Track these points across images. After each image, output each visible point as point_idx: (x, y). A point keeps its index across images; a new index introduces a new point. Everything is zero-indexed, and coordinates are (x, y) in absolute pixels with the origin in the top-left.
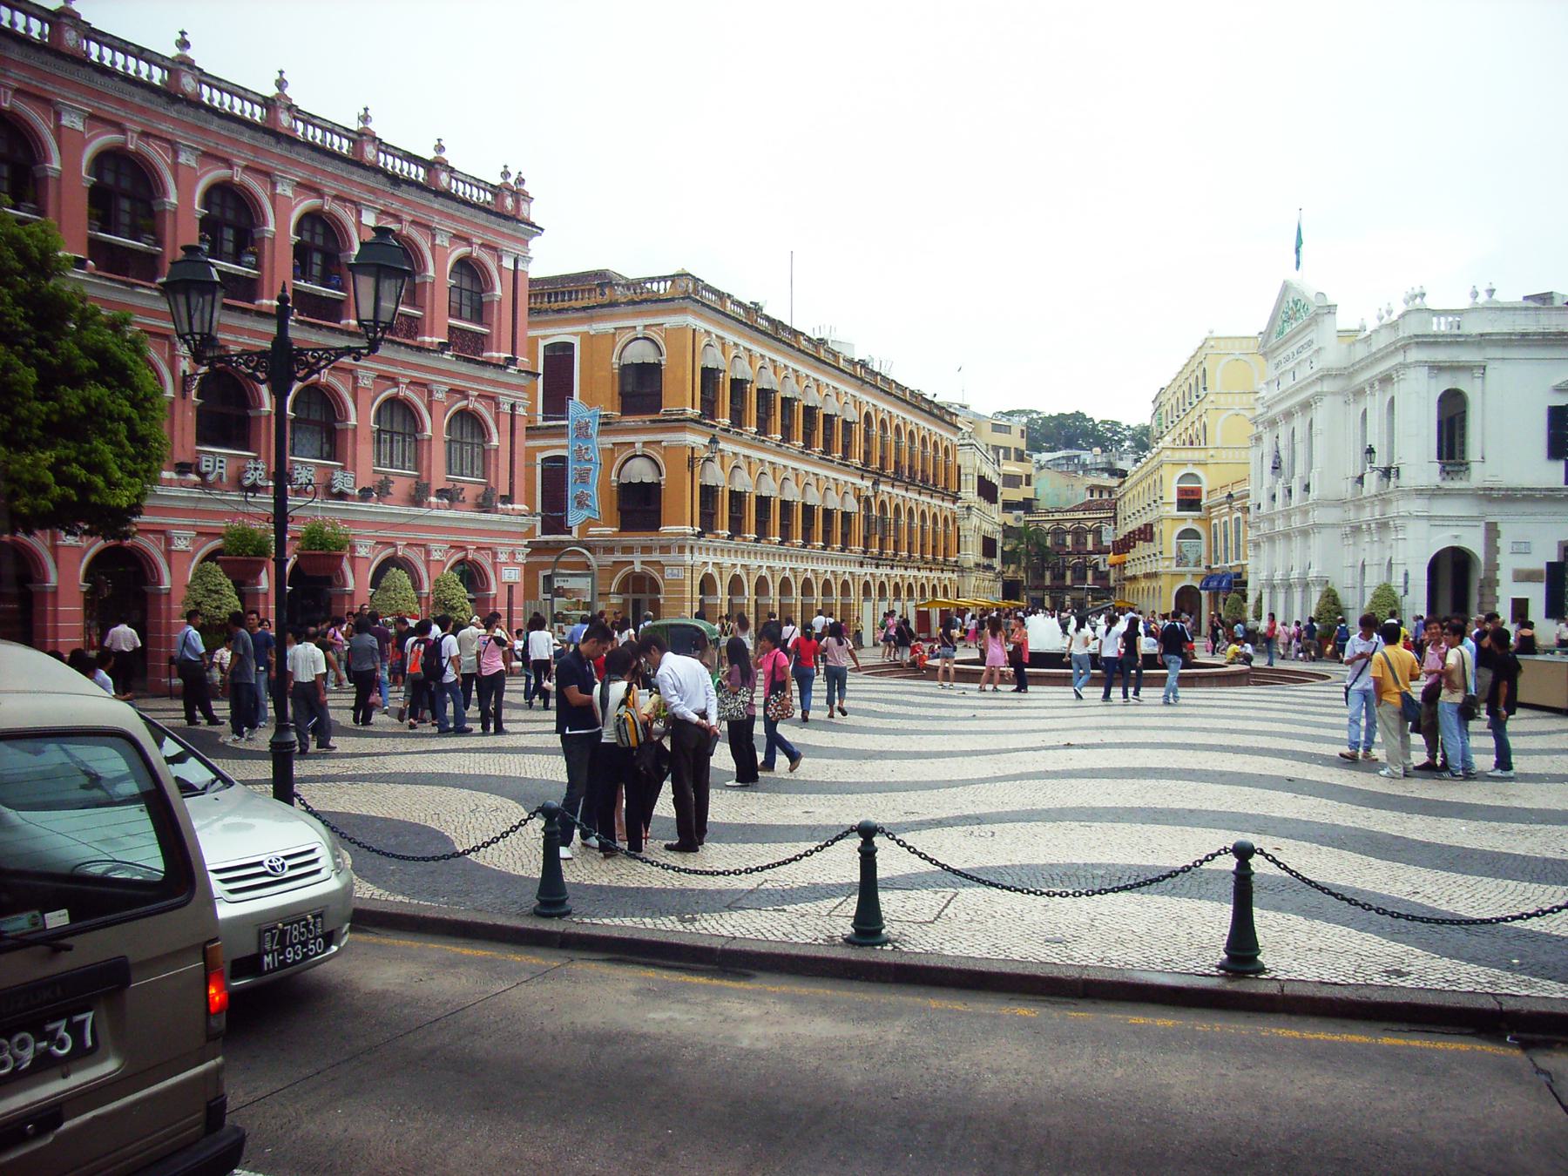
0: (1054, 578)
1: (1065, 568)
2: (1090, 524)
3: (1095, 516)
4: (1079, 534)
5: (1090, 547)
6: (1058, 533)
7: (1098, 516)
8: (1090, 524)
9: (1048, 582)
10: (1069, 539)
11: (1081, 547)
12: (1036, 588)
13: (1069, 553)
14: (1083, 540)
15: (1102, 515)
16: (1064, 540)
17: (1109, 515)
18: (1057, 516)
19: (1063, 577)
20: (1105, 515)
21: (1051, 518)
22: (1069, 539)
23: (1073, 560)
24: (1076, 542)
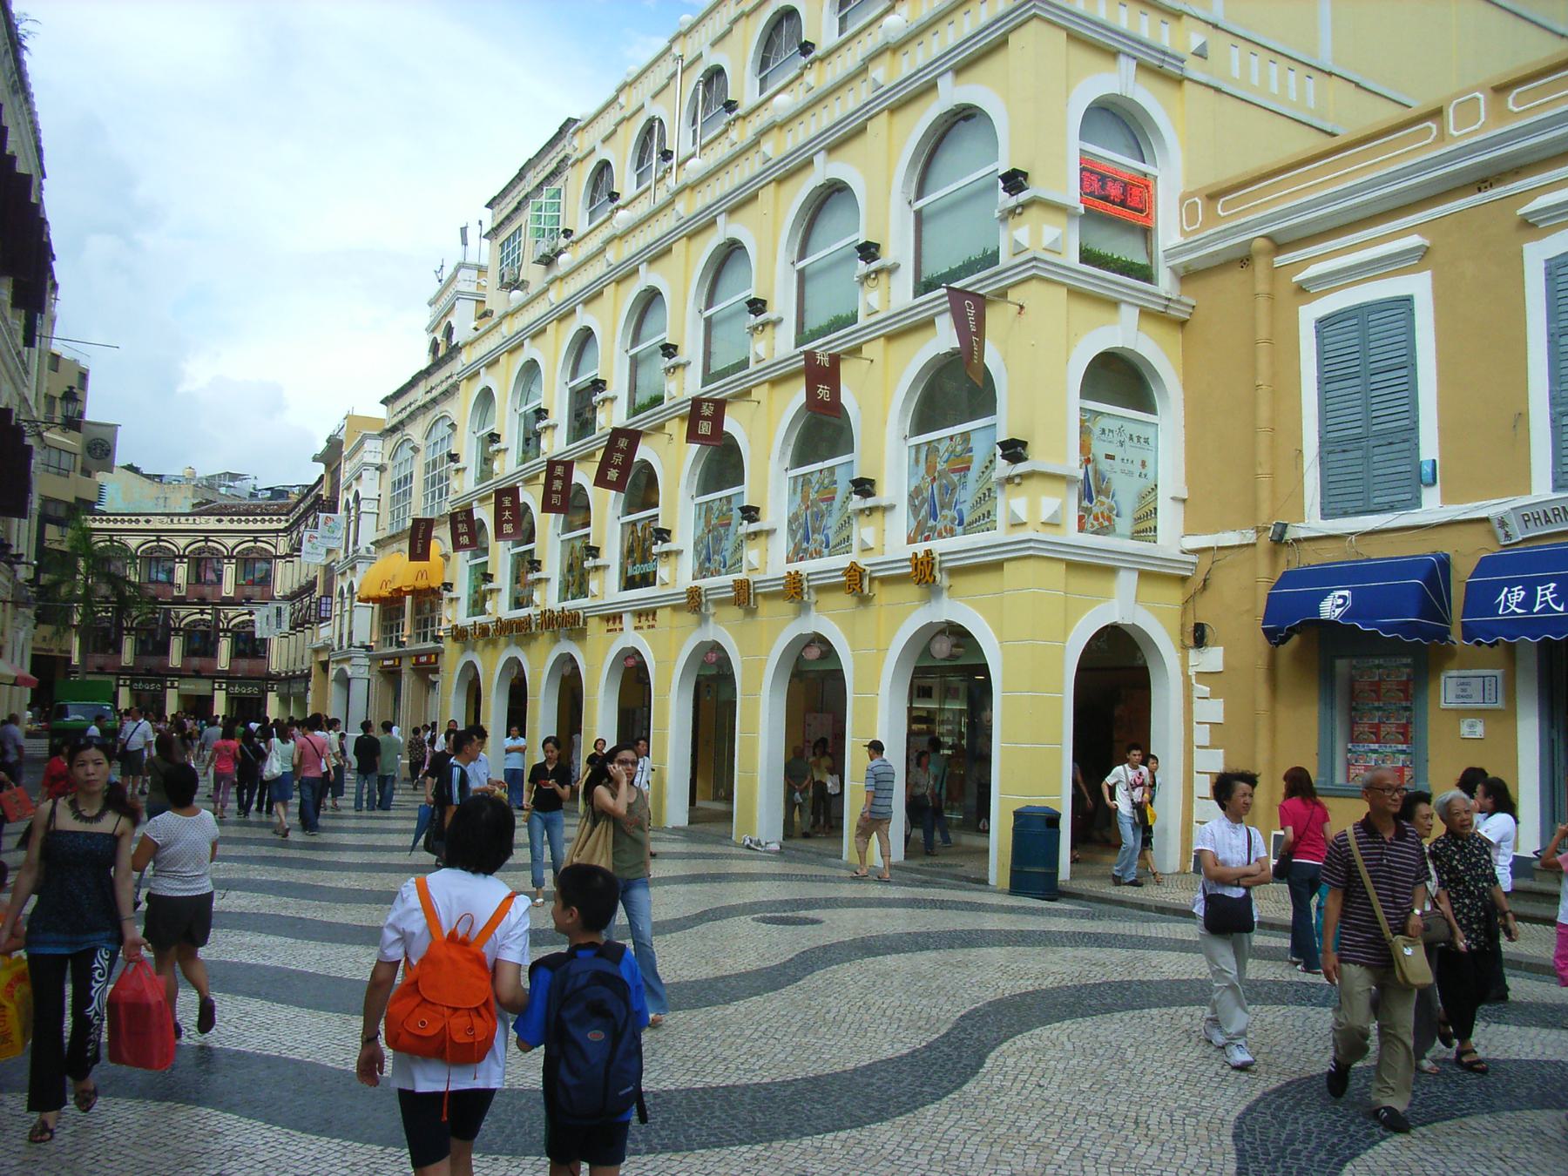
0: (141, 650)
1: (169, 631)
2: (230, 542)
3: (243, 526)
4: (203, 562)
5: (228, 589)
6: (159, 558)
7: (251, 526)
8: (230, 542)
9: (127, 657)
10: (181, 572)
11: (207, 590)
12: (198, 674)
13: (181, 601)
14: (211, 576)
15: (259, 526)
16: (171, 571)
17: (275, 526)
18: (156, 523)
19: (164, 649)
20: (267, 526)
21: (142, 525)
22: (181, 572)
23: (188, 615)
24: (197, 577)
